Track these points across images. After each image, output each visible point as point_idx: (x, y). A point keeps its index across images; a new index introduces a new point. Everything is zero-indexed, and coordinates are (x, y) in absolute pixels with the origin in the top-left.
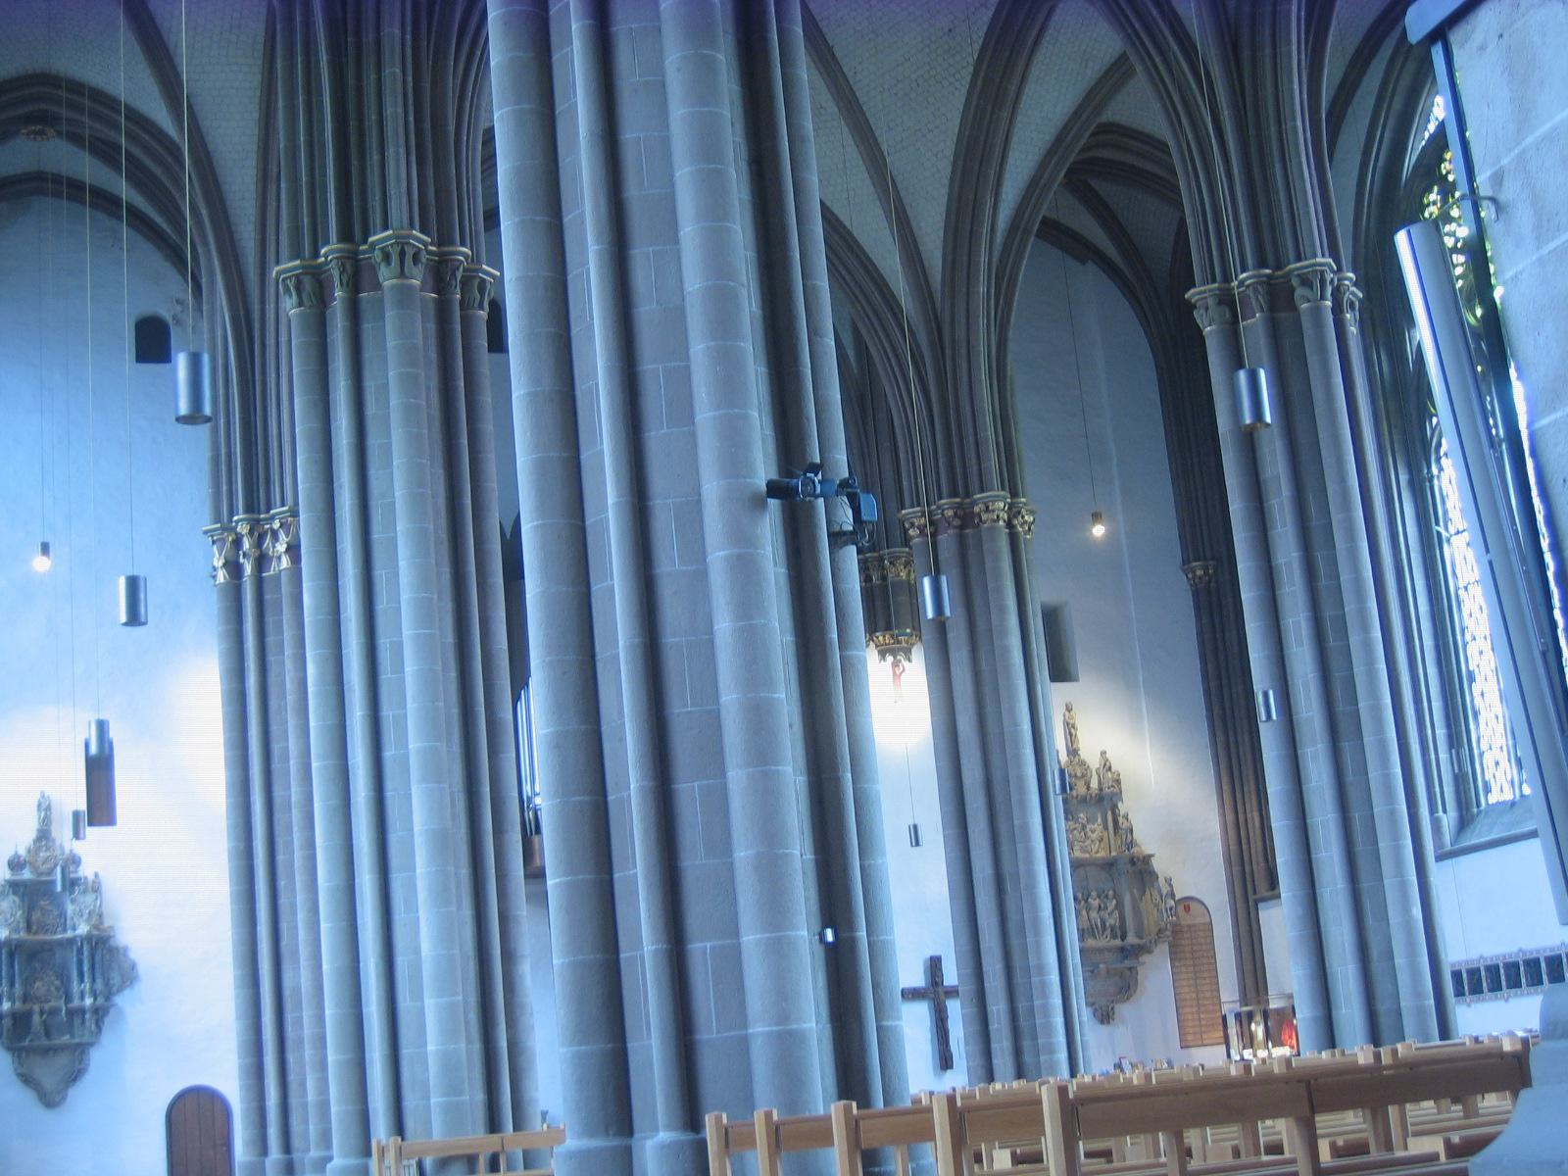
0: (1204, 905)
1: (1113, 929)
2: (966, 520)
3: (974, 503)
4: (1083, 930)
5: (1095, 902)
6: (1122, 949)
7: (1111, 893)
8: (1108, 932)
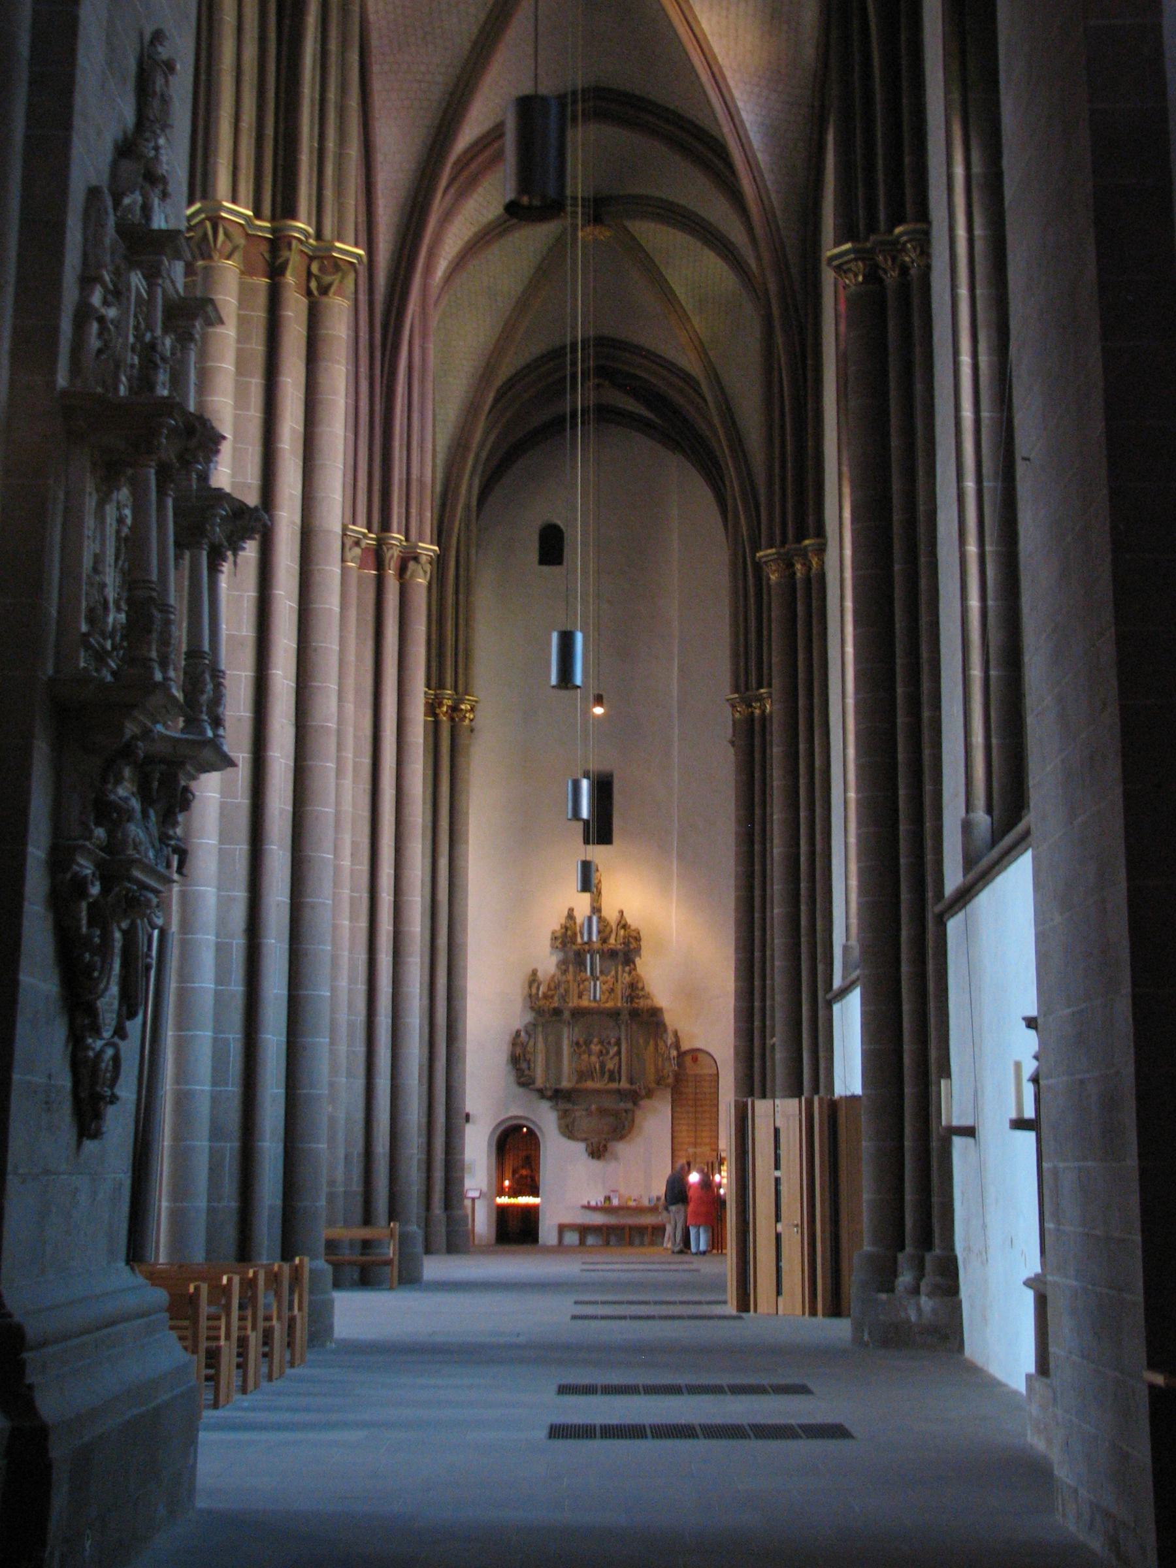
0: (712, 1057)
1: (611, 1073)
4: (582, 1072)
5: (595, 1048)
6: (619, 1092)
7: (613, 1040)
8: (607, 1076)
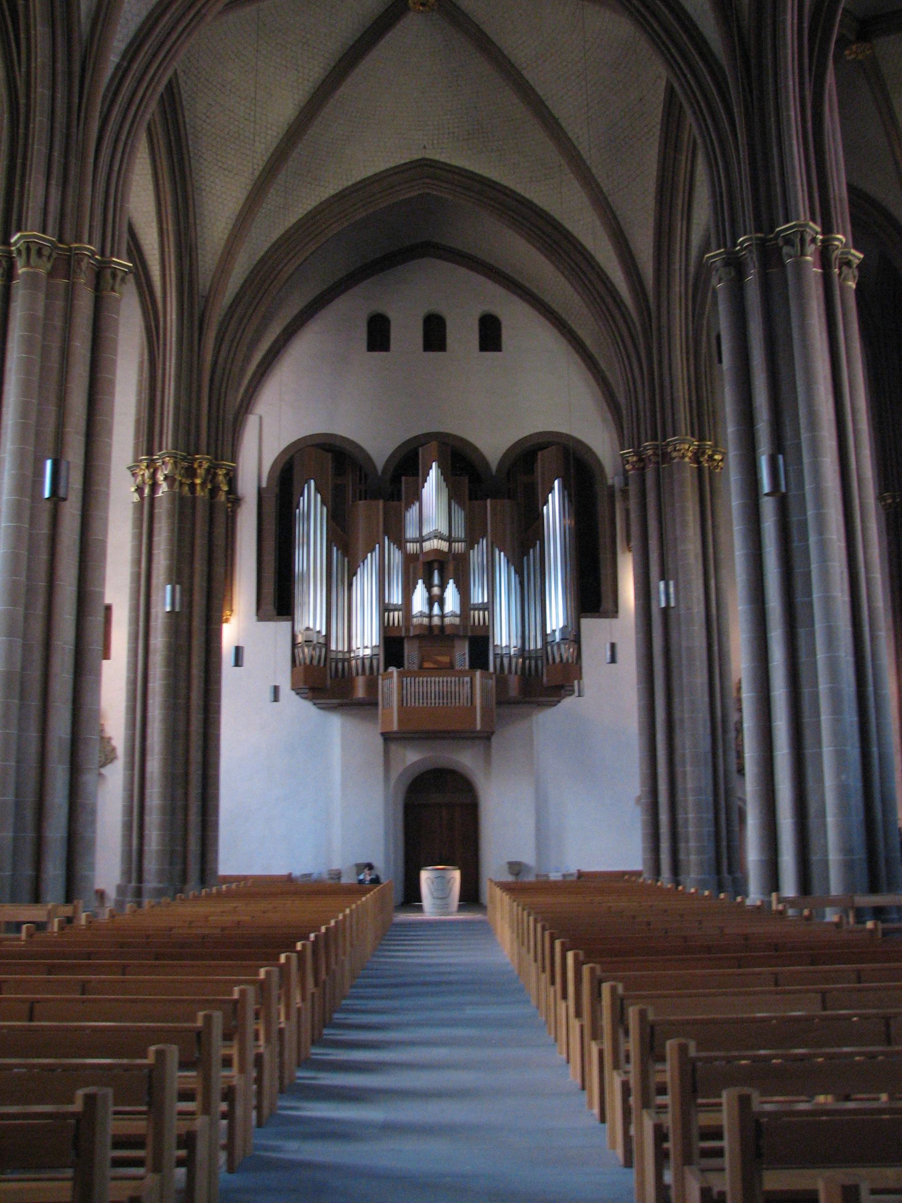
2: (664, 457)
3: (668, 444)
